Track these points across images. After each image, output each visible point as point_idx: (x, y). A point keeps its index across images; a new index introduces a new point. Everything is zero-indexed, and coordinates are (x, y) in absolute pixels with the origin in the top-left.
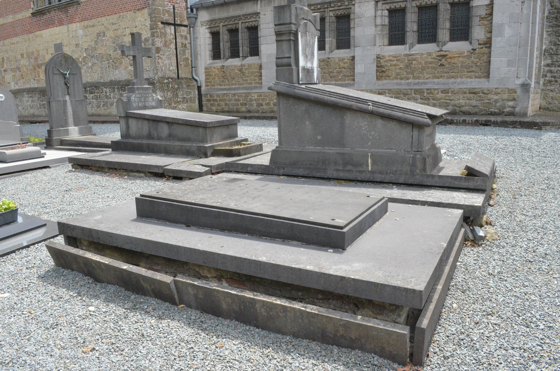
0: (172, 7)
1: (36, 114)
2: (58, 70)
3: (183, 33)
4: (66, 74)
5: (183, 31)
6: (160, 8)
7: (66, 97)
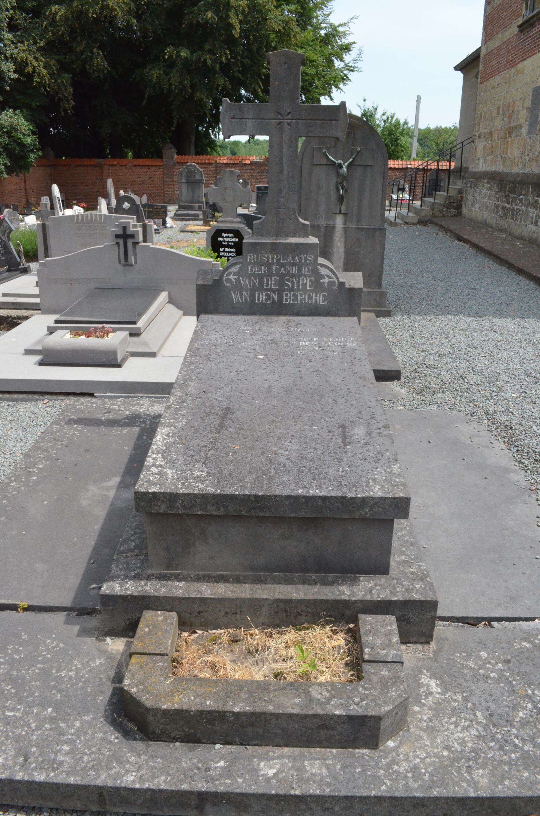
2: (325, 154)
4: (340, 166)
7: (334, 220)
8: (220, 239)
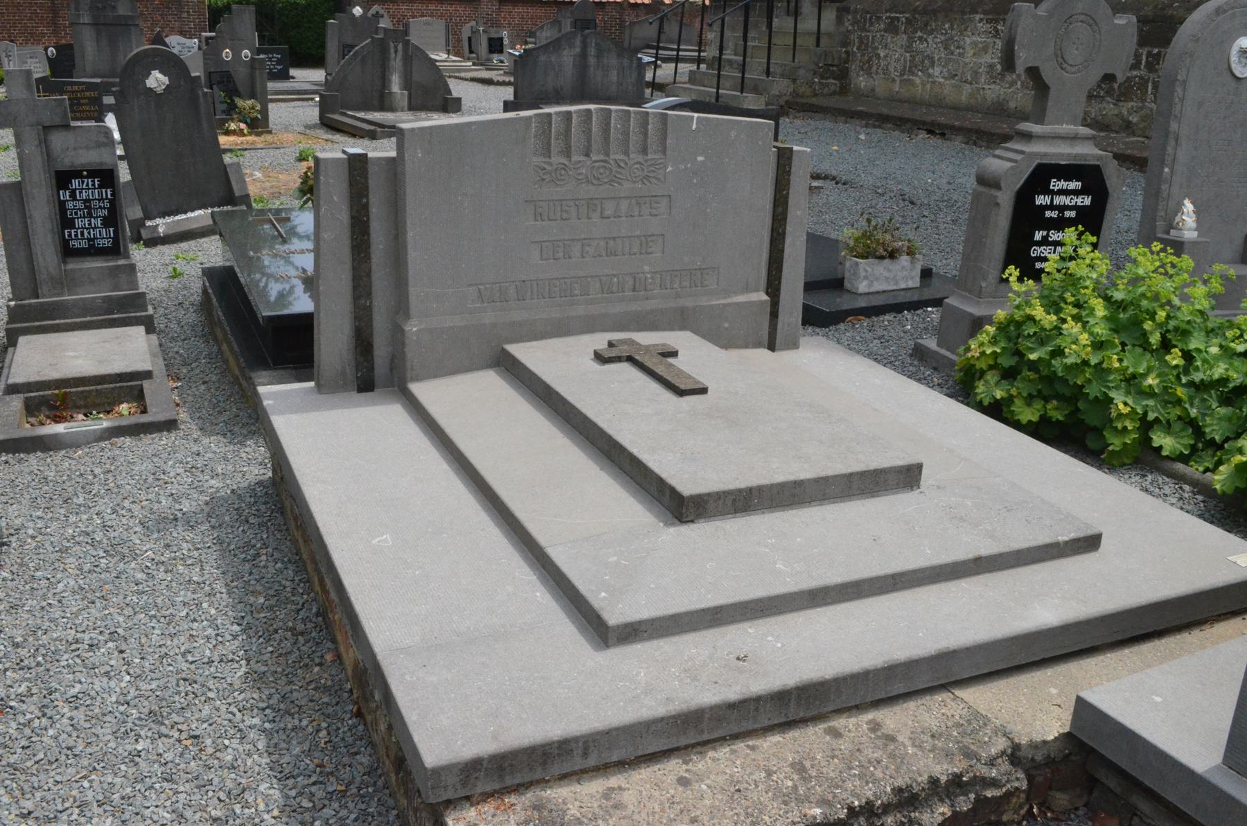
1: (1012, 105)
8: (1041, 200)
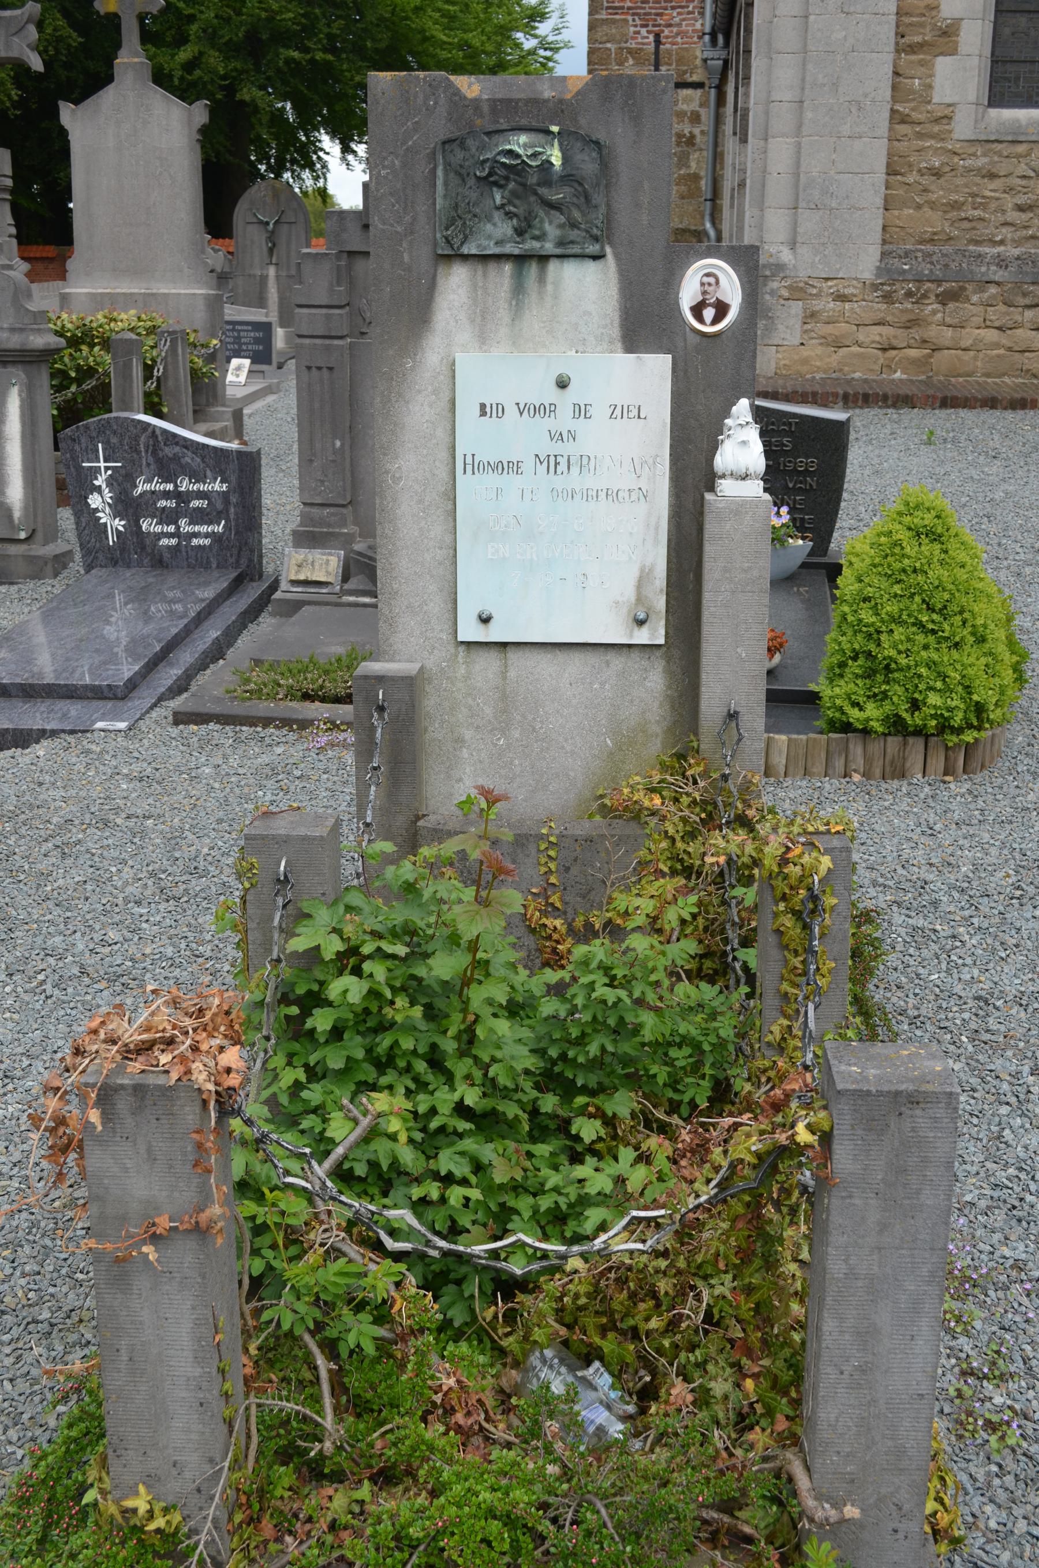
0: (651, 38)
3: (685, 107)
4: (267, 223)
5: (687, 100)
6: (609, 45)
